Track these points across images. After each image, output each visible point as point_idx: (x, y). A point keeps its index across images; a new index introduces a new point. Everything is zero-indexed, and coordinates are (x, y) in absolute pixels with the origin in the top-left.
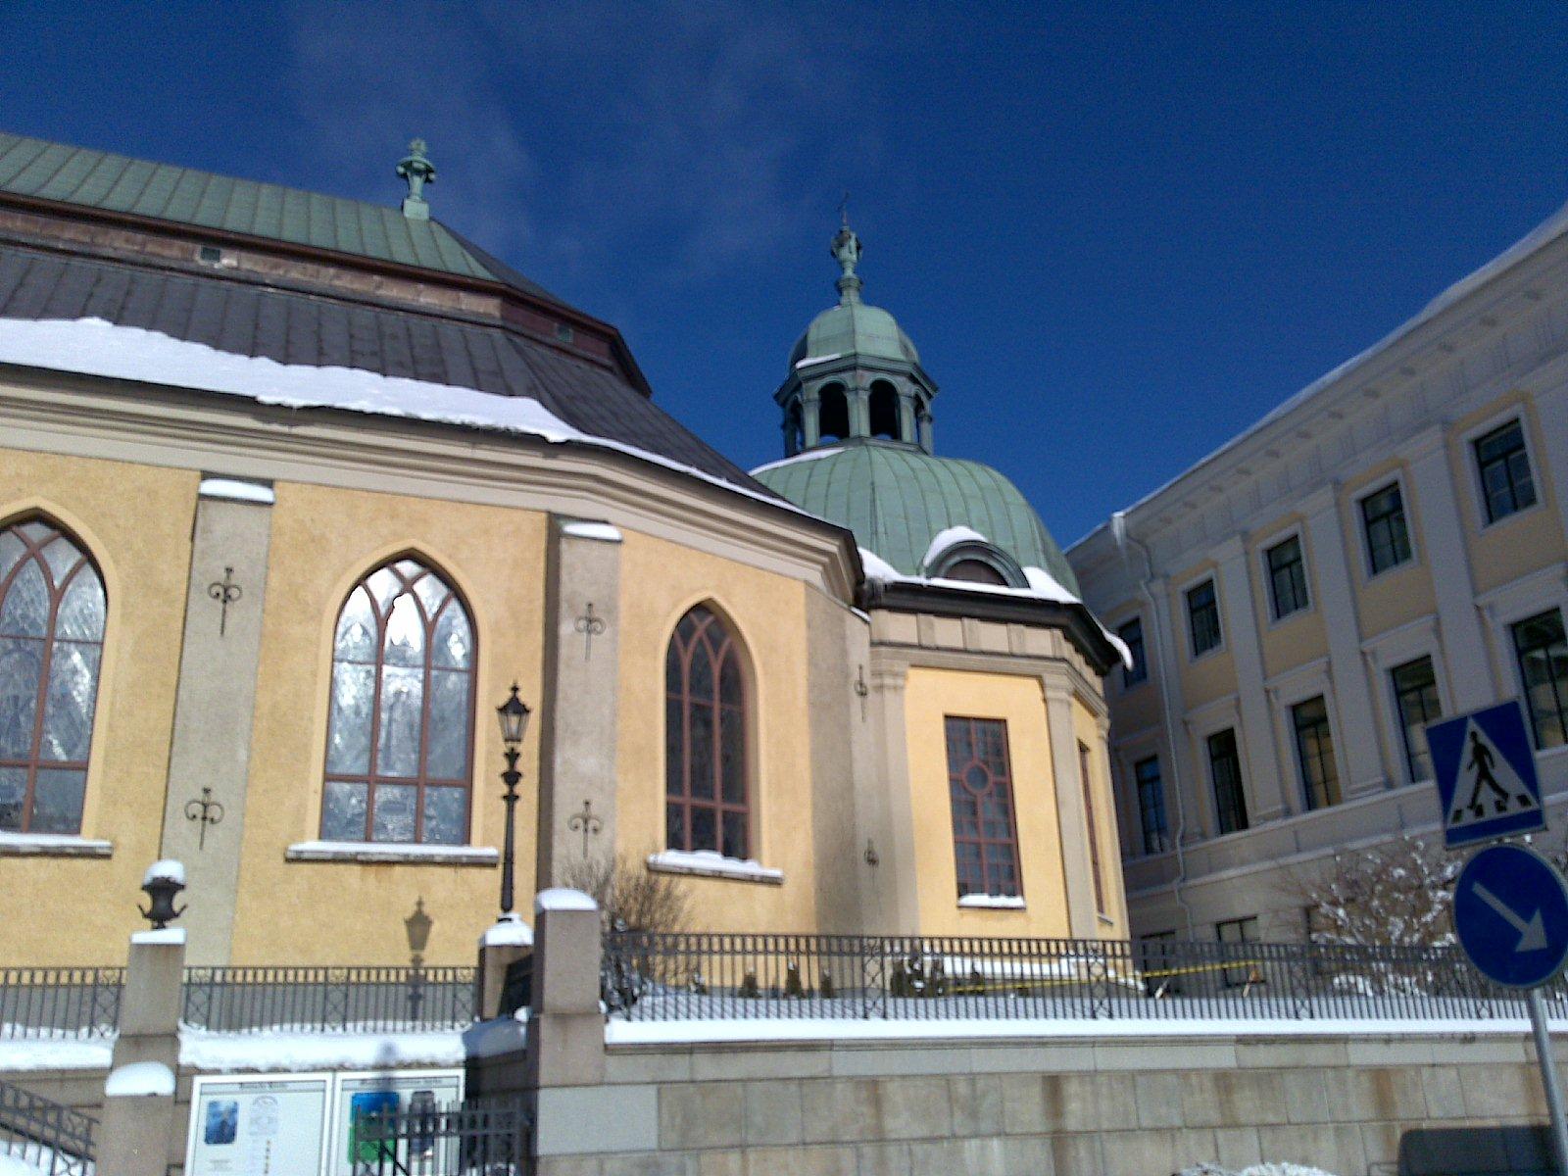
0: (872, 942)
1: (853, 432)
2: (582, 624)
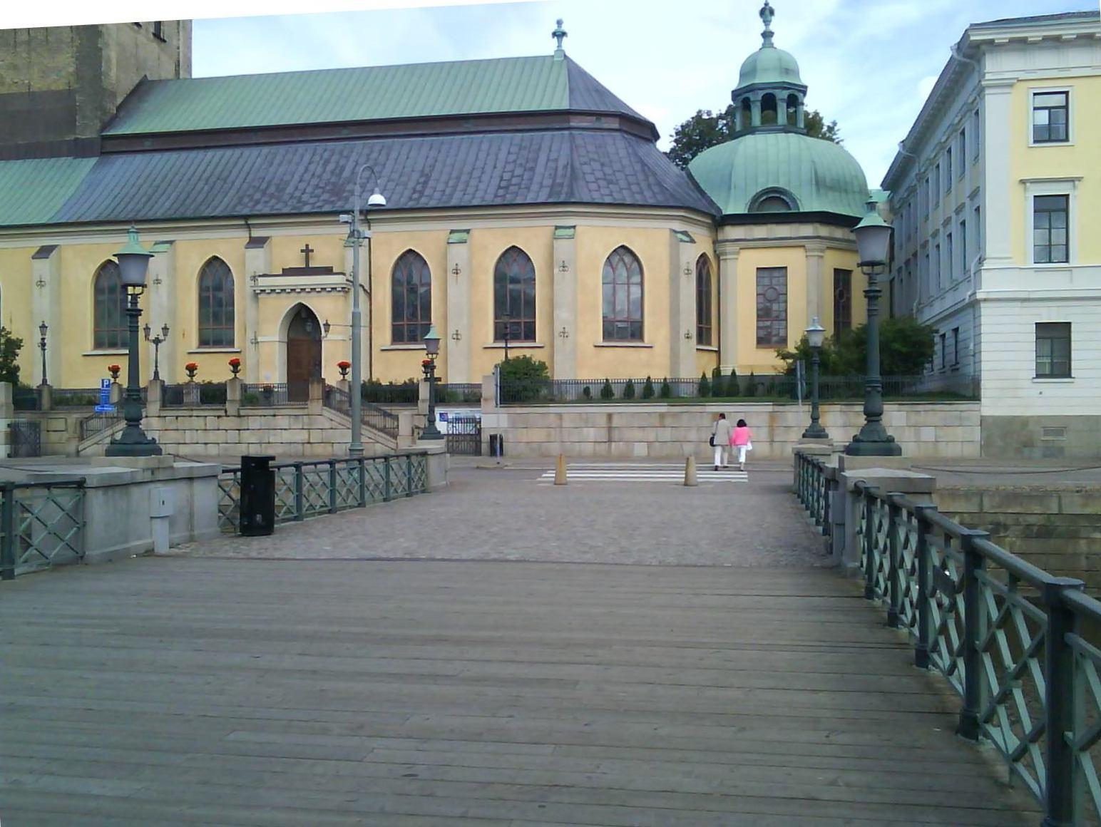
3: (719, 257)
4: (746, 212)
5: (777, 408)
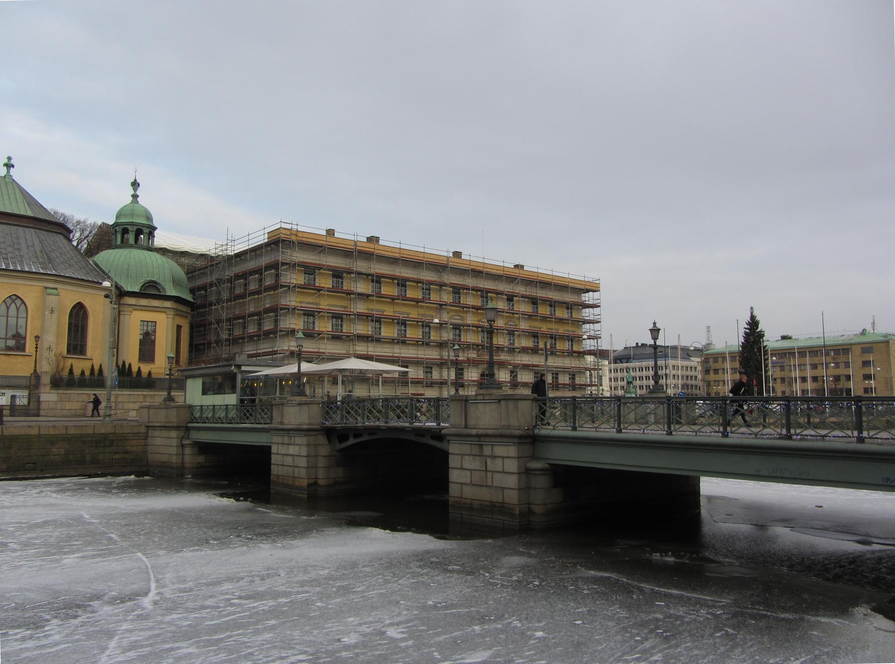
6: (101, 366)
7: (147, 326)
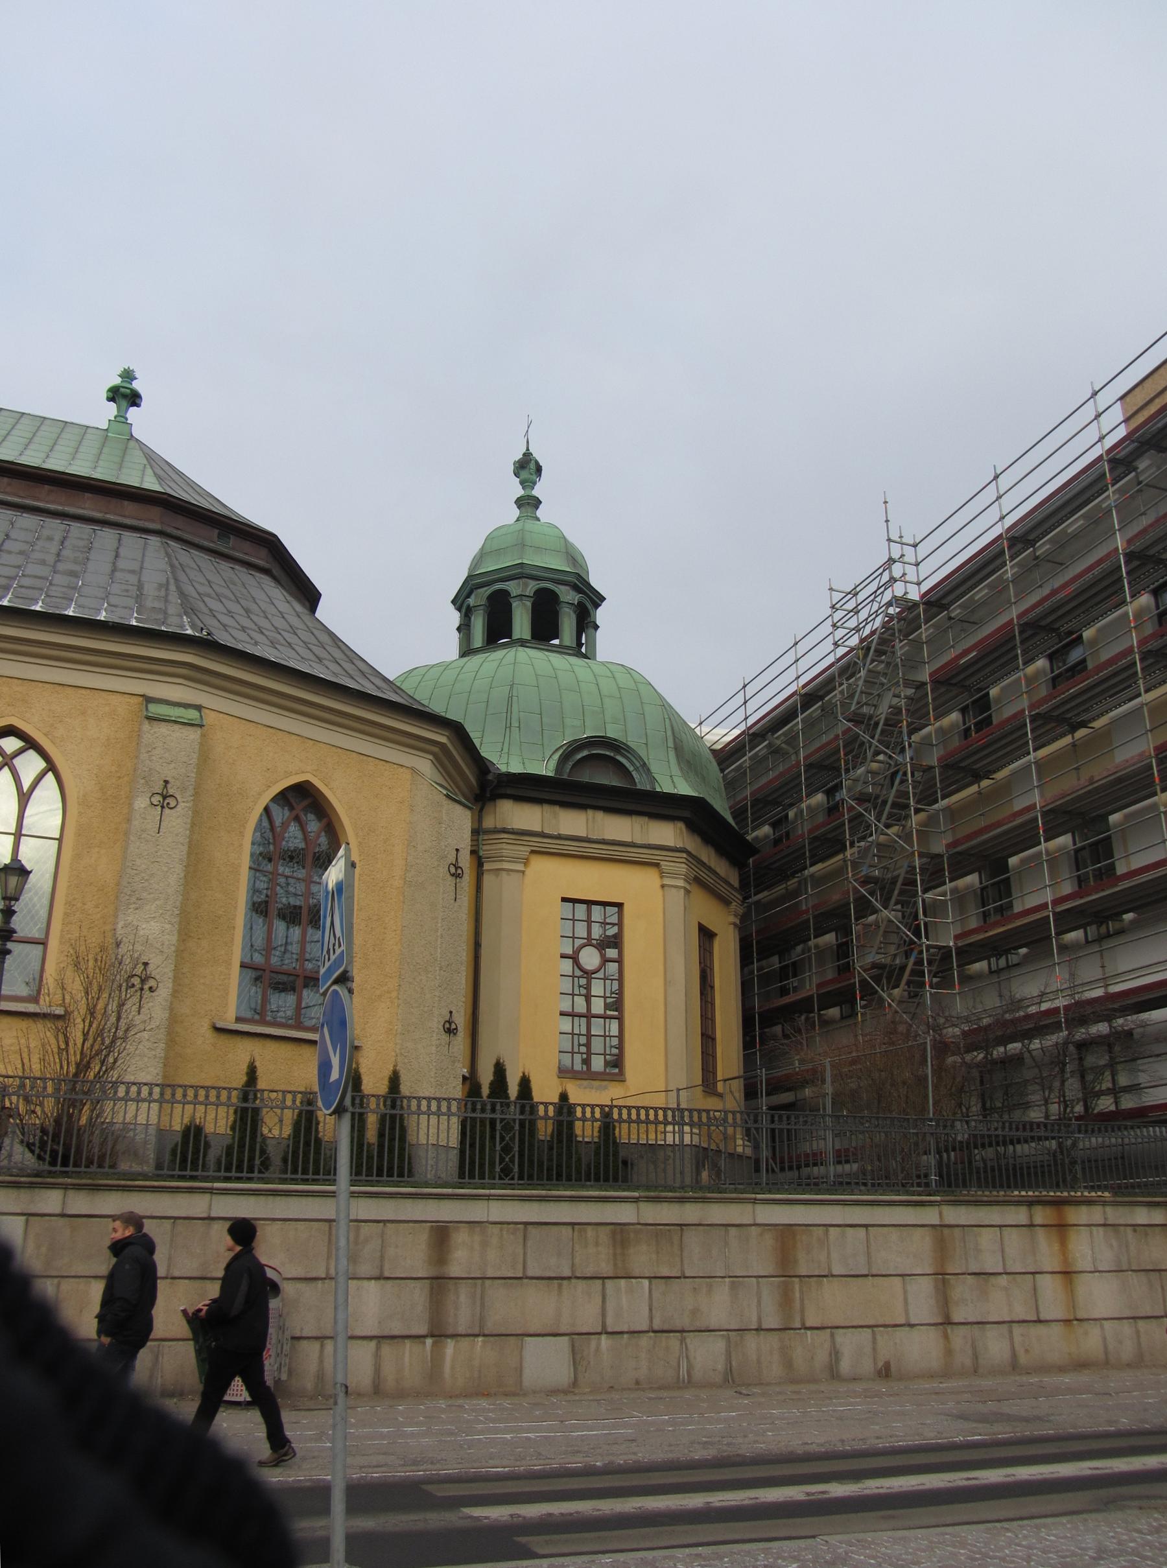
0: (273, 1095)
1: (516, 634)
2: (157, 799)
3: (480, 865)
4: (551, 774)
5: (956, 1215)
6: (394, 1081)
7: (589, 922)
